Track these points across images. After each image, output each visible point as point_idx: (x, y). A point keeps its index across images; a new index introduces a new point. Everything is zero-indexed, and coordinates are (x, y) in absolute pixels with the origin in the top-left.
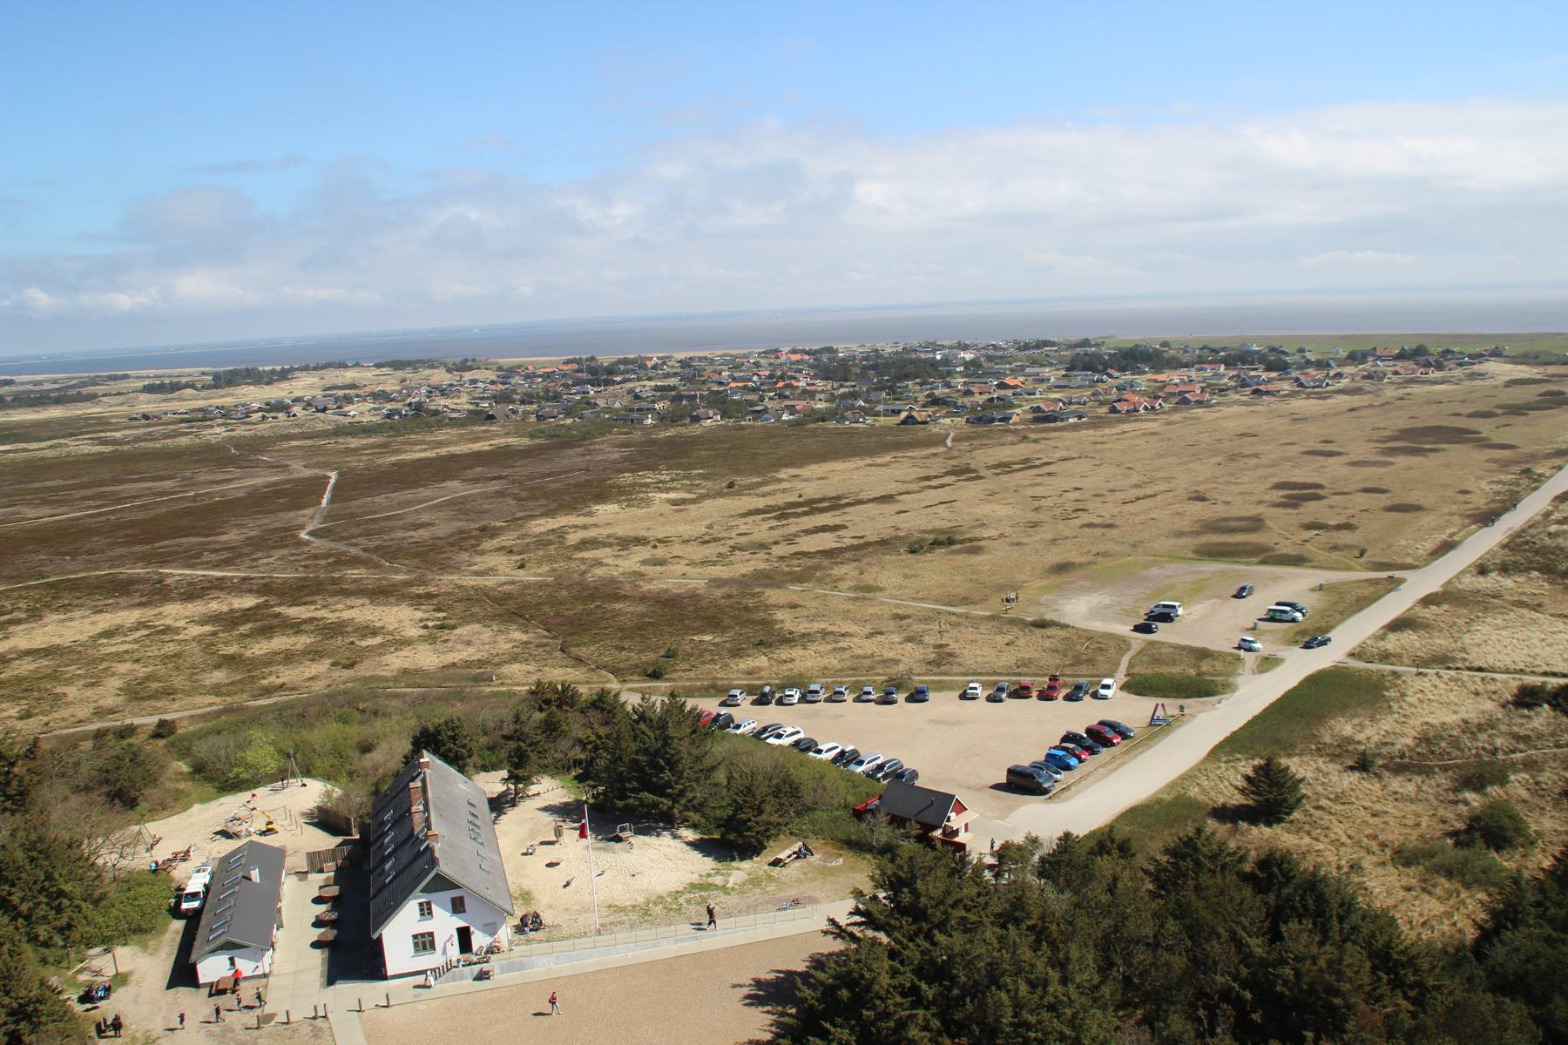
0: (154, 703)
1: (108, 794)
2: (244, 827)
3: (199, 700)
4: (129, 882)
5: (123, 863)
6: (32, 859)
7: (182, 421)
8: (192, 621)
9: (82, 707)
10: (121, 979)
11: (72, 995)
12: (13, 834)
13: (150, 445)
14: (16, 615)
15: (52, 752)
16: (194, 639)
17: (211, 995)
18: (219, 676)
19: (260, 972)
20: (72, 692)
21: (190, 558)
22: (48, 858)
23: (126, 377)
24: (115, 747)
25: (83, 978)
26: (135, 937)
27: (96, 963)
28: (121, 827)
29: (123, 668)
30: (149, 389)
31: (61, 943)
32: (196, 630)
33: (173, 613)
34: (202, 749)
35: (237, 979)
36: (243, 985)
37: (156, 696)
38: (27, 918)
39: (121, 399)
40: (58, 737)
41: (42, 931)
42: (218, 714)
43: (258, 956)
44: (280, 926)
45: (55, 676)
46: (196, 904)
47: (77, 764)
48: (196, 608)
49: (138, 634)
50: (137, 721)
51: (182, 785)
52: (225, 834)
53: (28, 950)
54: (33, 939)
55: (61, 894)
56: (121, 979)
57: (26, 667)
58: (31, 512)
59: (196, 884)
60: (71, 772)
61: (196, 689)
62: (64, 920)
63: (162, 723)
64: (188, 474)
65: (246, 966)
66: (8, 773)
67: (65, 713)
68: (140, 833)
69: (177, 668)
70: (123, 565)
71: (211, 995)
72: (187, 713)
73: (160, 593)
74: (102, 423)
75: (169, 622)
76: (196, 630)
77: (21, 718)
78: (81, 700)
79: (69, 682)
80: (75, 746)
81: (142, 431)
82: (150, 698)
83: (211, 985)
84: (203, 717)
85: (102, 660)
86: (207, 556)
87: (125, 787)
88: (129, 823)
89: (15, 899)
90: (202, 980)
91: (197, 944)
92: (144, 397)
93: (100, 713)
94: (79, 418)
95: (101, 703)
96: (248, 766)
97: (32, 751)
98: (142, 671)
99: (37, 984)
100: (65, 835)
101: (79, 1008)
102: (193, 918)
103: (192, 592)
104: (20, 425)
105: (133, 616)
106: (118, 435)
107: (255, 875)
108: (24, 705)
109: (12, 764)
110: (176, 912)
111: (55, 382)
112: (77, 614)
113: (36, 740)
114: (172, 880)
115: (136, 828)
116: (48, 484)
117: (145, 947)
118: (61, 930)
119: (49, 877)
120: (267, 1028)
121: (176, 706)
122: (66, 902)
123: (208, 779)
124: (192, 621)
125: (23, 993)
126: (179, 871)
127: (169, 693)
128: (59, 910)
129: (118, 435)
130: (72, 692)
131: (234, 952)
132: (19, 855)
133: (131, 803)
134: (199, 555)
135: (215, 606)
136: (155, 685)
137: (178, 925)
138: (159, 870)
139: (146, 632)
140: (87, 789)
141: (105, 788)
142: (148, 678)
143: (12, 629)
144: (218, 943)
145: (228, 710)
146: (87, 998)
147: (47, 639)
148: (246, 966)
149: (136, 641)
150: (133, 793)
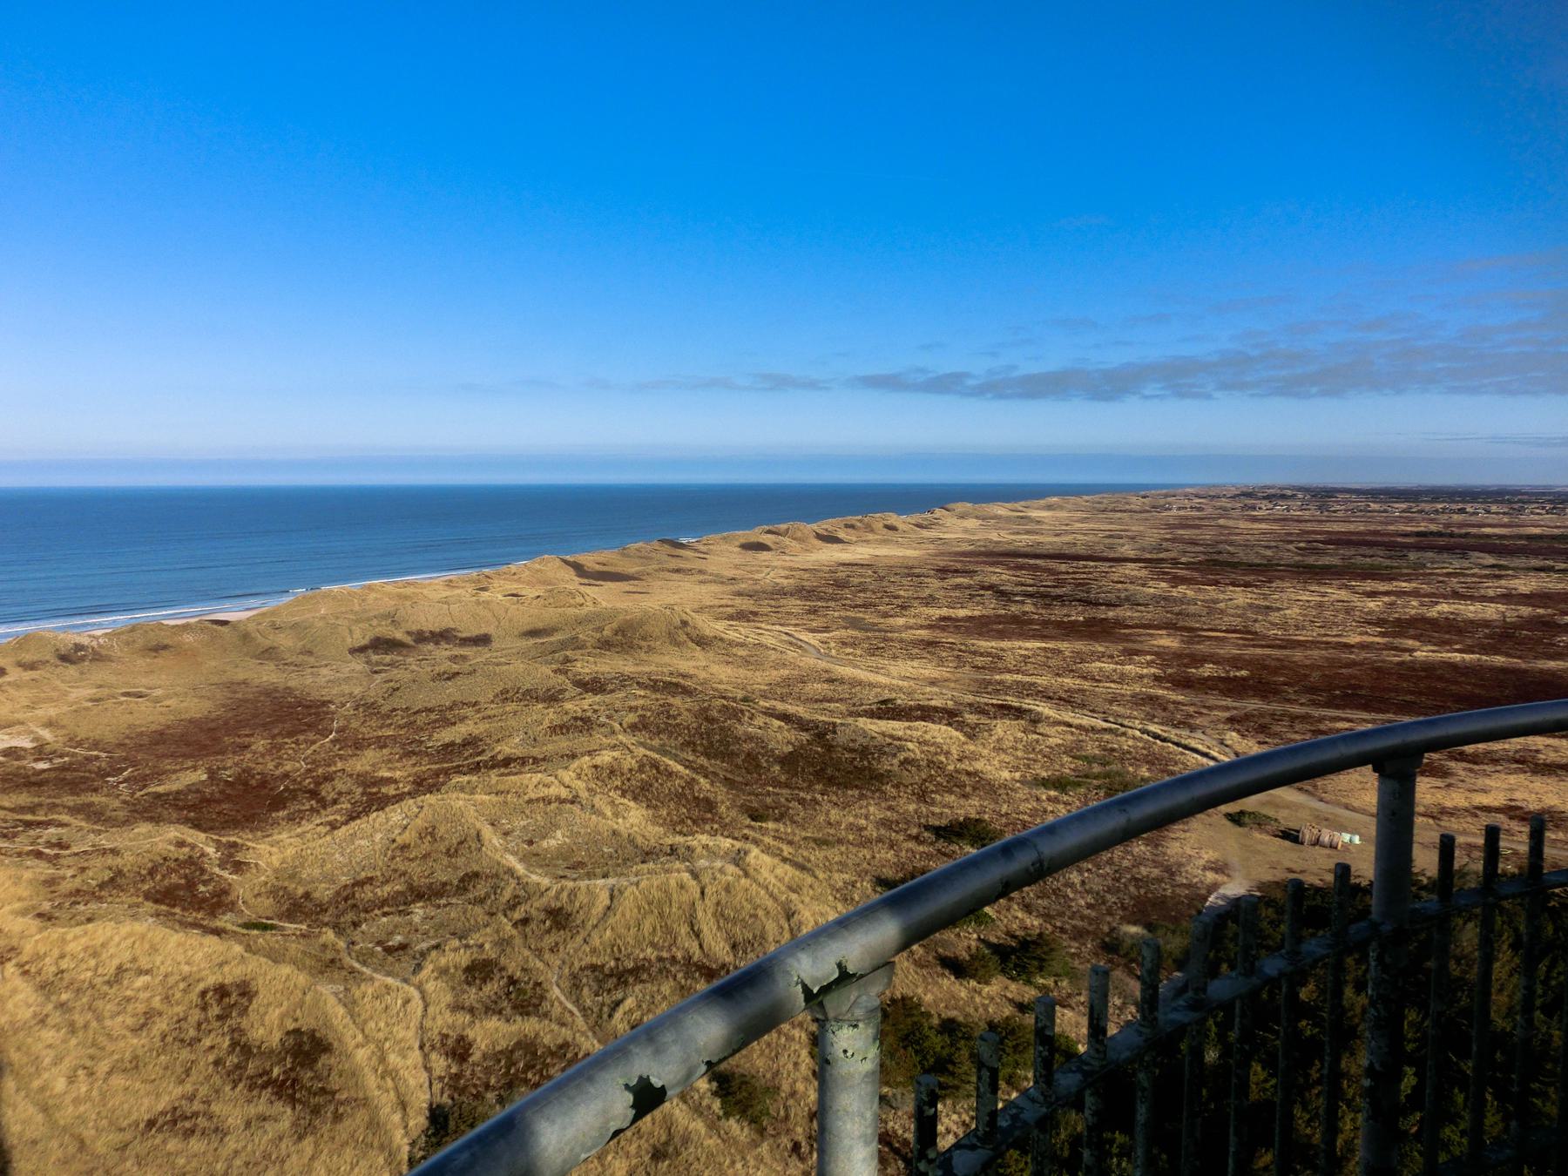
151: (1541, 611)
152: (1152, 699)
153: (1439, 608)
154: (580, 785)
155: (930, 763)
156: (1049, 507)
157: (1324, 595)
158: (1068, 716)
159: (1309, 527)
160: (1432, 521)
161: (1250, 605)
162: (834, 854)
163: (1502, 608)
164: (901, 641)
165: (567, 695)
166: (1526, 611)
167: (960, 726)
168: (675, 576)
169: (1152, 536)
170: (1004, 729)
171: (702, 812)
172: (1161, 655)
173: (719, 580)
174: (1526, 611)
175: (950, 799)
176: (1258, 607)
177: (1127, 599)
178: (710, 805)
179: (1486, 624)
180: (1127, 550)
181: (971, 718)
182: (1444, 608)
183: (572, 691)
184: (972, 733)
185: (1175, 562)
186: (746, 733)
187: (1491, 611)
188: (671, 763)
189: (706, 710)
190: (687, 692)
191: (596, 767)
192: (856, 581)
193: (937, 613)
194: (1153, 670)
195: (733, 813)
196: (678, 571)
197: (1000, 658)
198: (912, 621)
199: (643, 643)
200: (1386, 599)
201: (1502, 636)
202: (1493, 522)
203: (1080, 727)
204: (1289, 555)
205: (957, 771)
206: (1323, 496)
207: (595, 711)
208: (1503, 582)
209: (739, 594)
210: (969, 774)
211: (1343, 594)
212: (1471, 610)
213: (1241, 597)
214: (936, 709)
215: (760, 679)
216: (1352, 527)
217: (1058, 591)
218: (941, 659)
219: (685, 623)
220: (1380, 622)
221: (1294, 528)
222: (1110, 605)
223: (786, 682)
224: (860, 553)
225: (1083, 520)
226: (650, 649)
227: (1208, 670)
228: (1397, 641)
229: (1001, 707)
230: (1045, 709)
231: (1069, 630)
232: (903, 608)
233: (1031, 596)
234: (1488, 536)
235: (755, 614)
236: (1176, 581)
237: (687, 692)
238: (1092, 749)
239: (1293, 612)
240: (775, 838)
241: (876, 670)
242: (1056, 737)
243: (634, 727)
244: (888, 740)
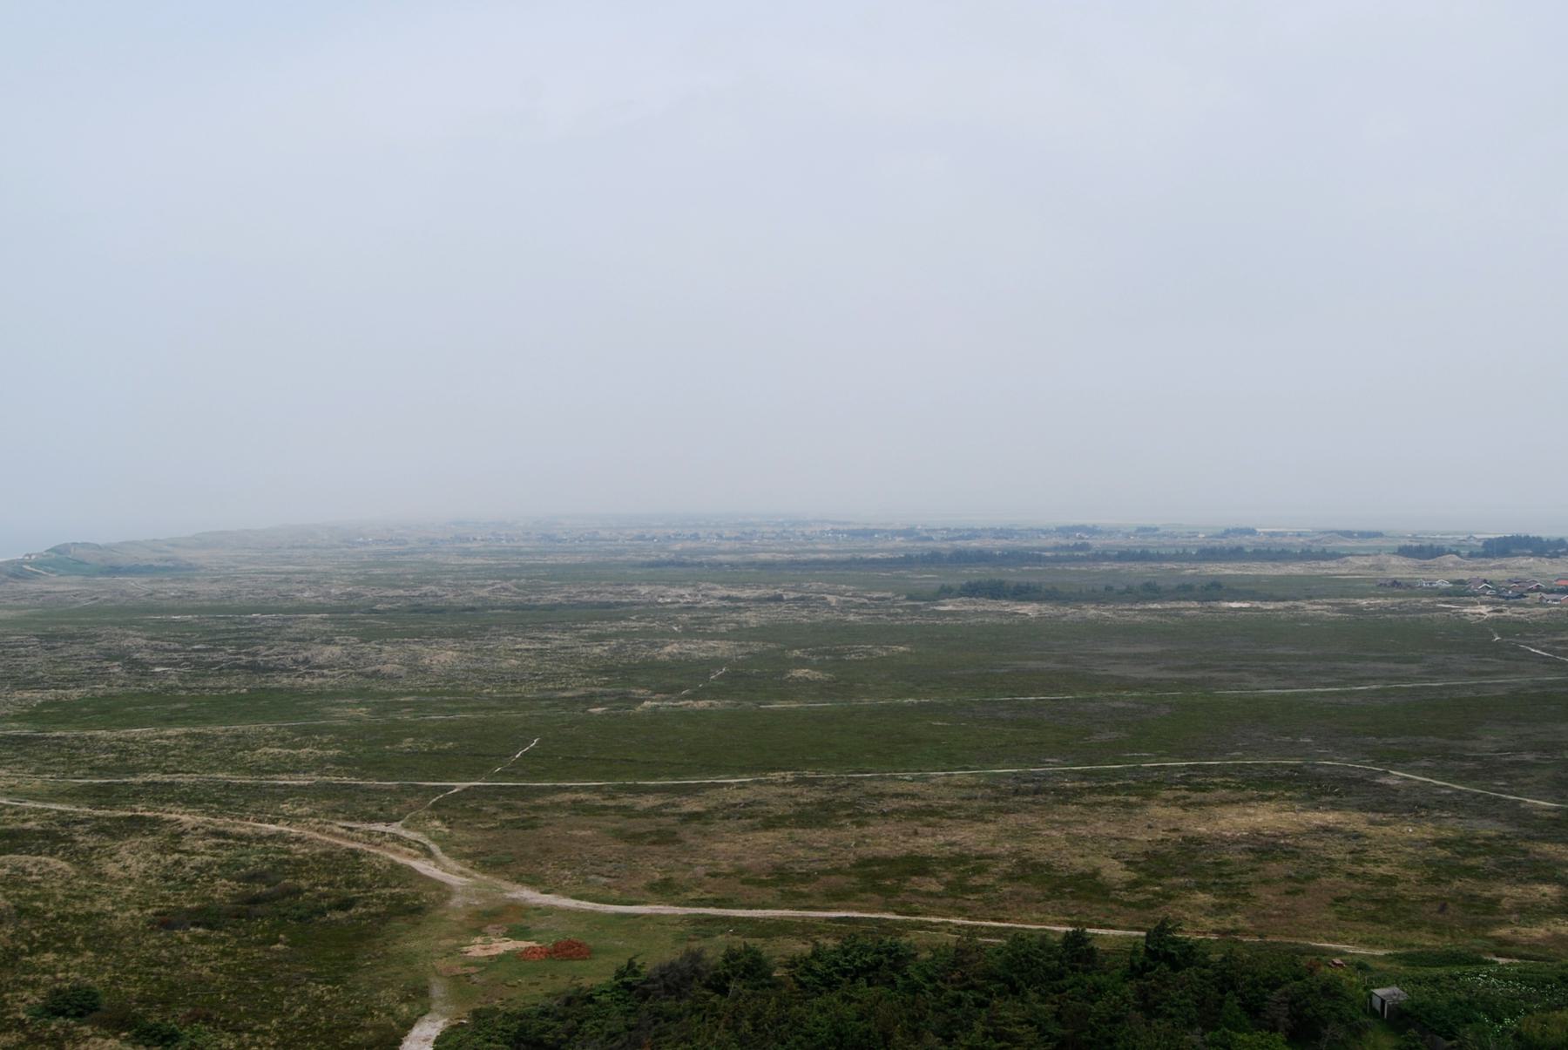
153: (668, 649)
155: (22, 912)
157: (545, 641)
181: (85, 840)
184: (83, 859)
200: (614, 643)
205: (64, 918)
210: (77, 919)
220: (607, 671)
242: (202, 852)
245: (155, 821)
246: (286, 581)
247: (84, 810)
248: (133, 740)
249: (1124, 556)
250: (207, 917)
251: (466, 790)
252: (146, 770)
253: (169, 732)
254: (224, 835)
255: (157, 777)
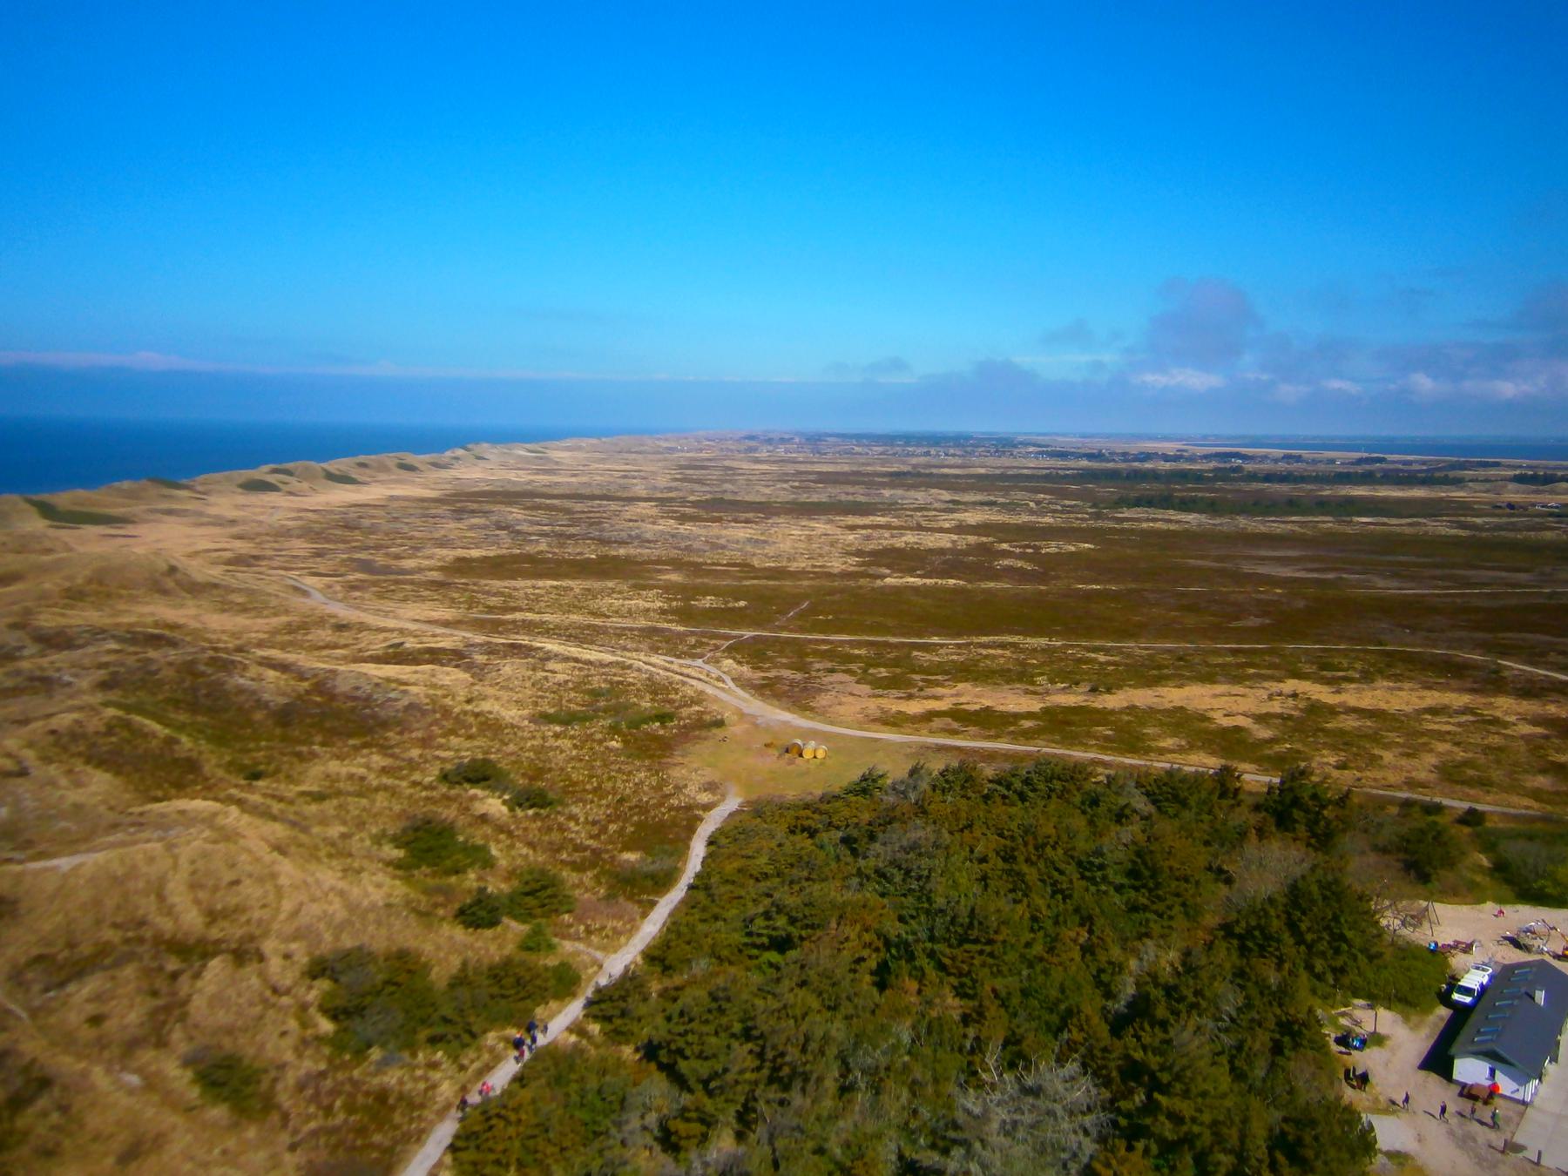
0: (1467, 790)
1: (1405, 861)
2: (1537, 943)
3: (1515, 799)
4: (1408, 952)
5: (1406, 932)
6: (1325, 898)
7: (1551, 515)
8: (1524, 719)
9: (1394, 774)
10: (1377, 1039)
11: (1331, 1033)
12: (1313, 869)
13: (1511, 535)
14: (1351, 673)
15: (1361, 807)
16: (1522, 737)
17: (1461, 1095)
18: (1542, 781)
19: (1519, 1096)
20: (1388, 756)
21: (1534, 656)
22: (1339, 901)
23: (1497, 464)
24: (1419, 821)
25: (1343, 1021)
26: (1400, 1006)
27: (1358, 1014)
28: (1410, 898)
29: (1442, 747)
30: (1520, 479)
31: (1331, 981)
32: (1527, 729)
33: (1505, 706)
34: (1511, 850)
35: (1493, 1091)
36: (1497, 1101)
37: (1469, 782)
38: (1310, 947)
39: (1488, 485)
40: (1368, 794)
41: (1319, 965)
42: (1532, 820)
43: (1523, 1080)
44: (1554, 1059)
45: (1375, 738)
46: (1468, 1000)
47: (1381, 825)
48: (1530, 707)
49: (1464, 718)
50: (1446, 802)
51: (1478, 878)
52: (1515, 943)
53: (1304, 976)
54: (1309, 967)
55: (1343, 938)
56: (1377, 1039)
57: (1350, 723)
58: (1381, 583)
59: (1474, 979)
60: (1372, 830)
61: (1515, 788)
62: (1338, 963)
63: (1471, 811)
64: (1548, 569)
65: (1506, 1085)
66: (1318, 813)
67: (1378, 774)
68: (1426, 909)
69: (1498, 762)
70: (1461, 648)
71: (1461, 1095)
72: (1498, 809)
73: (1494, 683)
74: (1465, 508)
75: (1498, 714)
76: (1527, 729)
77: (1337, 767)
78: (1395, 768)
79: (1387, 746)
80: (1382, 808)
81: (1504, 520)
82: (1463, 783)
83: (1464, 1086)
84: (1515, 818)
85: (1423, 734)
86: (1552, 657)
87: (1424, 858)
88: (1419, 897)
89: (1303, 927)
90: (1456, 1076)
91: (1461, 1039)
92: (1511, 486)
93: (1411, 784)
94: (1441, 499)
95: (1414, 774)
96: (1557, 883)
97: (1344, 800)
98: (1461, 755)
99: (1305, 1009)
100: (1358, 887)
101: (1335, 1048)
102: (1461, 1014)
103: (1529, 690)
104: (1385, 500)
105: (1465, 699)
106: (1478, 521)
107: (1540, 996)
108: (1342, 756)
109: (1323, 807)
110: (1445, 999)
111: (1424, 463)
112: (1407, 685)
113: (1349, 792)
114: (1448, 965)
115: (1424, 904)
116: (1402, 558)
117: (1406, 1019)
118: (1334, 970)
119: (1336, 918)
120: (1512, 1157)
121: (1488, 798)
122: (1345, 947)
123: (1509, 881)
124: (1524, 719)
125: (1292, 1011)
126: (1457, 960)
127: (1484, 783)
128: (1337, 951)
129: (1478, 521)
130: (1388, 756)
131: (1498, 1064)
132: (1315, 889)
133: (1424, 878)
134: (1543, 654)
135: (1552, 709)
136: (1470, 772)
137: (1443, 1012)
138: (1438, 953)
139: (1471, 718)
140: (1384, 851)
141: (1402, 856)
142: (1466, 763)
143: (1344, 685)
144: (1483, 1048)
145: (1546, 819)
146: (1343, 1040)
147: (1374, 702)
148: (1506, 1085)
149: (1459, 725)
150: (1428, 869)
151: (984, 539)
152: (654, 631)
154: (30, 755)
156: (568, 449)
158: (574, 651)
159: (802, 468)
160: (904, 463)
161: (749, 540)
162: (329, 806)
163: (955, 537)
164: (412, 582)
165: (26, 652)
166: (972, 539)
167: (469, 667)
168: (166, 518)
169: (662, 481)
170: (509, 667)
171: (181, 775)
172: (668, 588)
173: (220, 522)
174: (972, 539)
175: (454, 741)
176: (757, 541)
177: (638, 537)
178: (192, 765)
179: (942, 551)
180: (640, 490)
181: (480, 658)
182: (910, 538)
183: (32, 649)
184: (479, 672)
185: (683, 502)
186: (237, 686)
187: (945, 541)
188: (147, 722)
189: (193, 662)
190: (173, 644)
191: (53, 732)
192: (366, 522)
193: (450, 554)
194: (659, 604)
195: (220, 773)
196: (170, 512)
197: (510, 596)
198: (427, 562)
199: (124, 592)
201: (951, 563)
202: (950, 463)
203: (589, 663)
204: (782, 493)
205: (465, 713)
206: (814, 441)
207: (59, 670)
208: (956, 516)
209: (240, 537)
211: (829, 528)
212: (931, 541)
213: (740, 532)
214: (443, 650)
215: (255, 626)
216: (838, 468)
217: (572, 530)
218: (453, 600)
219: (173, 570)
220: (859, 553)
221: (790, 469)
222: (622, 543)
223: (290, 629)
224: (373, 493)
225: (602, 461)
226: (133, 599)
227: (708, 602)
228: (872, 570)
229: (513, 646)
230: (552, 646)
231: (581, 568)
232: (417, 549)
233: (545, 535)
234: (947, 476)
235: (256, 558)
236: (683, 519)
237: (173, 644)
238: (597, 682)
239: (786, 546)
240: (265, 795)
241: (386, 614)
242: (561, 673)
243: (104, 686)
244: (394, 685)
245: (531, 649)
246: (625, 477)
247: (479, 639)
248: (515, 589)
249: (1269, 478)
250: (567, 719)
251: (754, 638)
252: (520, 610)
253: (540, 583)
254: (576, 660)
255: (530, 616)
